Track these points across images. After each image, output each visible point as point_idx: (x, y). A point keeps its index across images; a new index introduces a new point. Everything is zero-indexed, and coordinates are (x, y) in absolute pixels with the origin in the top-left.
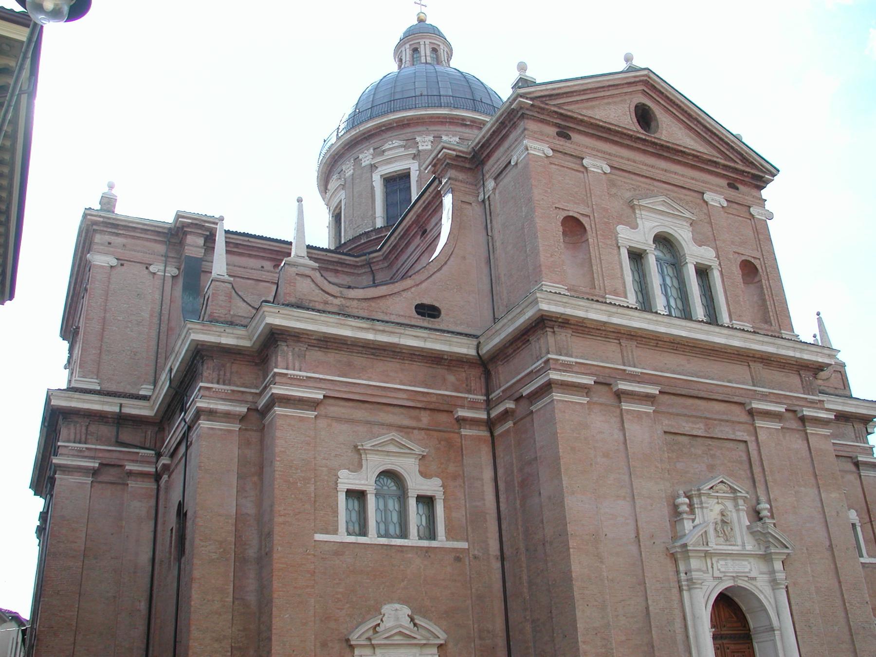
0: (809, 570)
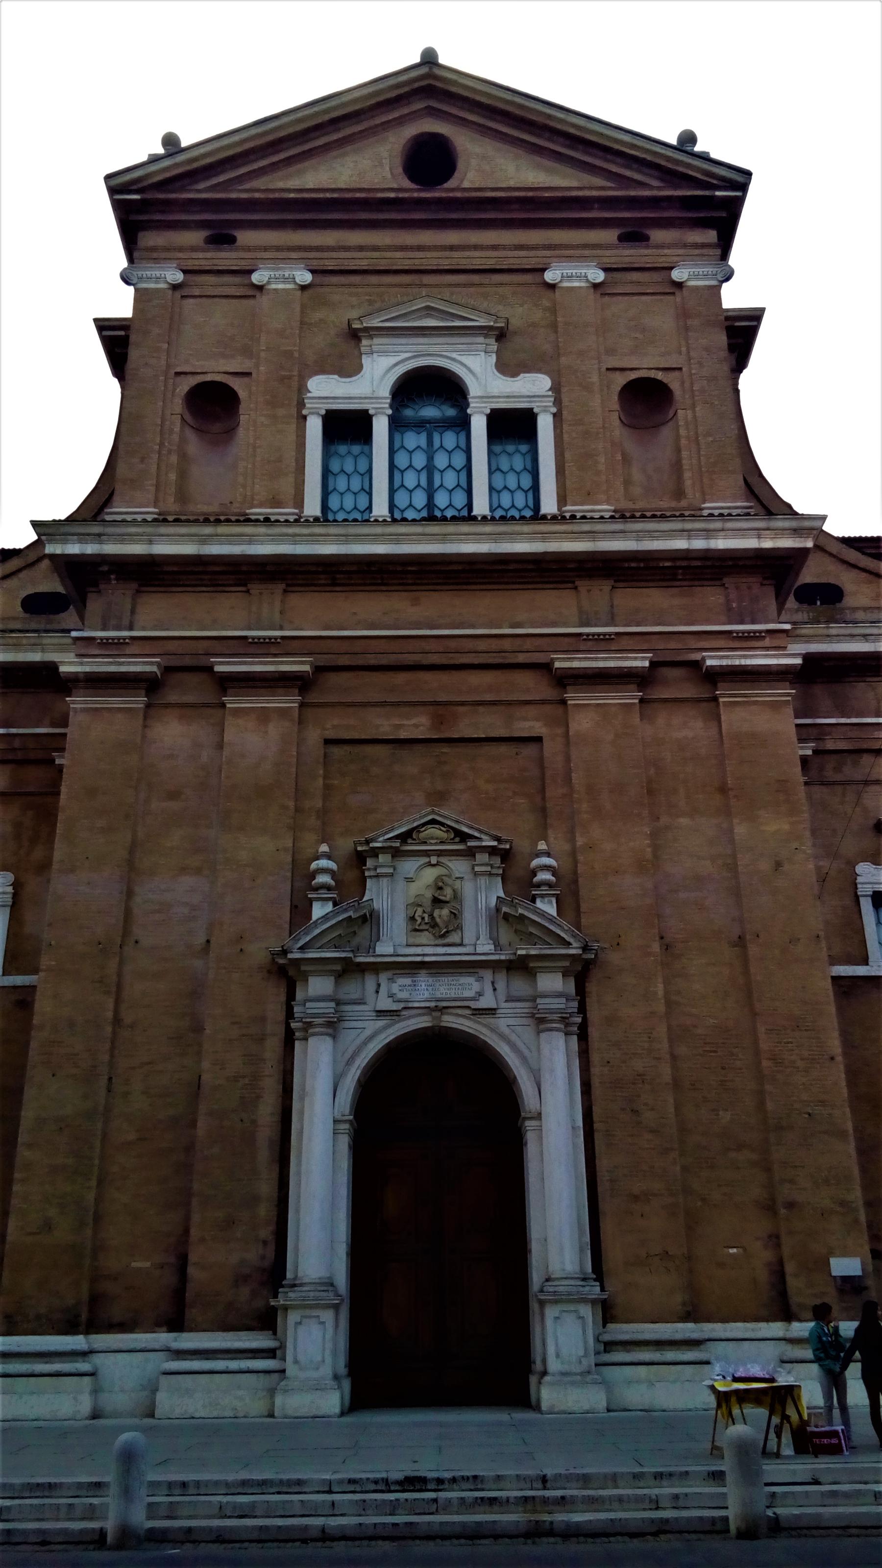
0: (660, 989)
